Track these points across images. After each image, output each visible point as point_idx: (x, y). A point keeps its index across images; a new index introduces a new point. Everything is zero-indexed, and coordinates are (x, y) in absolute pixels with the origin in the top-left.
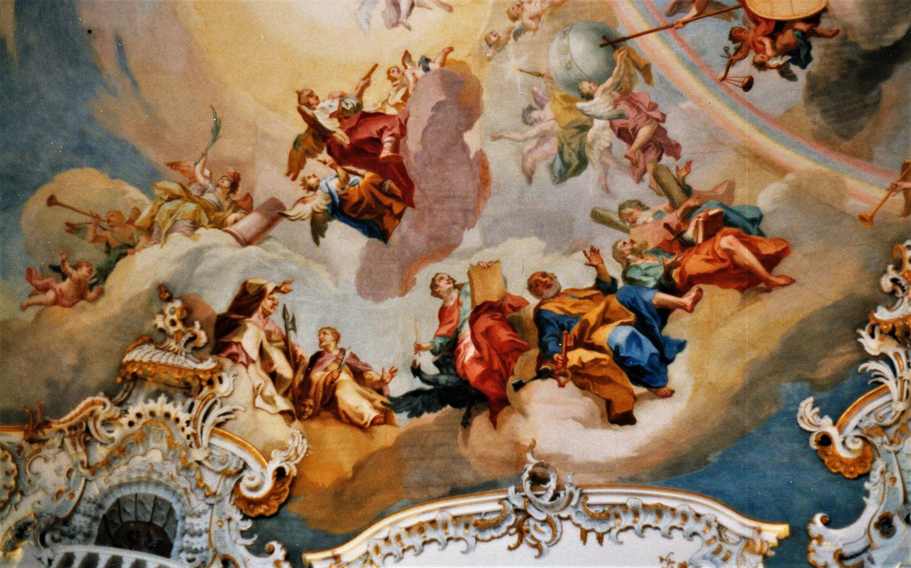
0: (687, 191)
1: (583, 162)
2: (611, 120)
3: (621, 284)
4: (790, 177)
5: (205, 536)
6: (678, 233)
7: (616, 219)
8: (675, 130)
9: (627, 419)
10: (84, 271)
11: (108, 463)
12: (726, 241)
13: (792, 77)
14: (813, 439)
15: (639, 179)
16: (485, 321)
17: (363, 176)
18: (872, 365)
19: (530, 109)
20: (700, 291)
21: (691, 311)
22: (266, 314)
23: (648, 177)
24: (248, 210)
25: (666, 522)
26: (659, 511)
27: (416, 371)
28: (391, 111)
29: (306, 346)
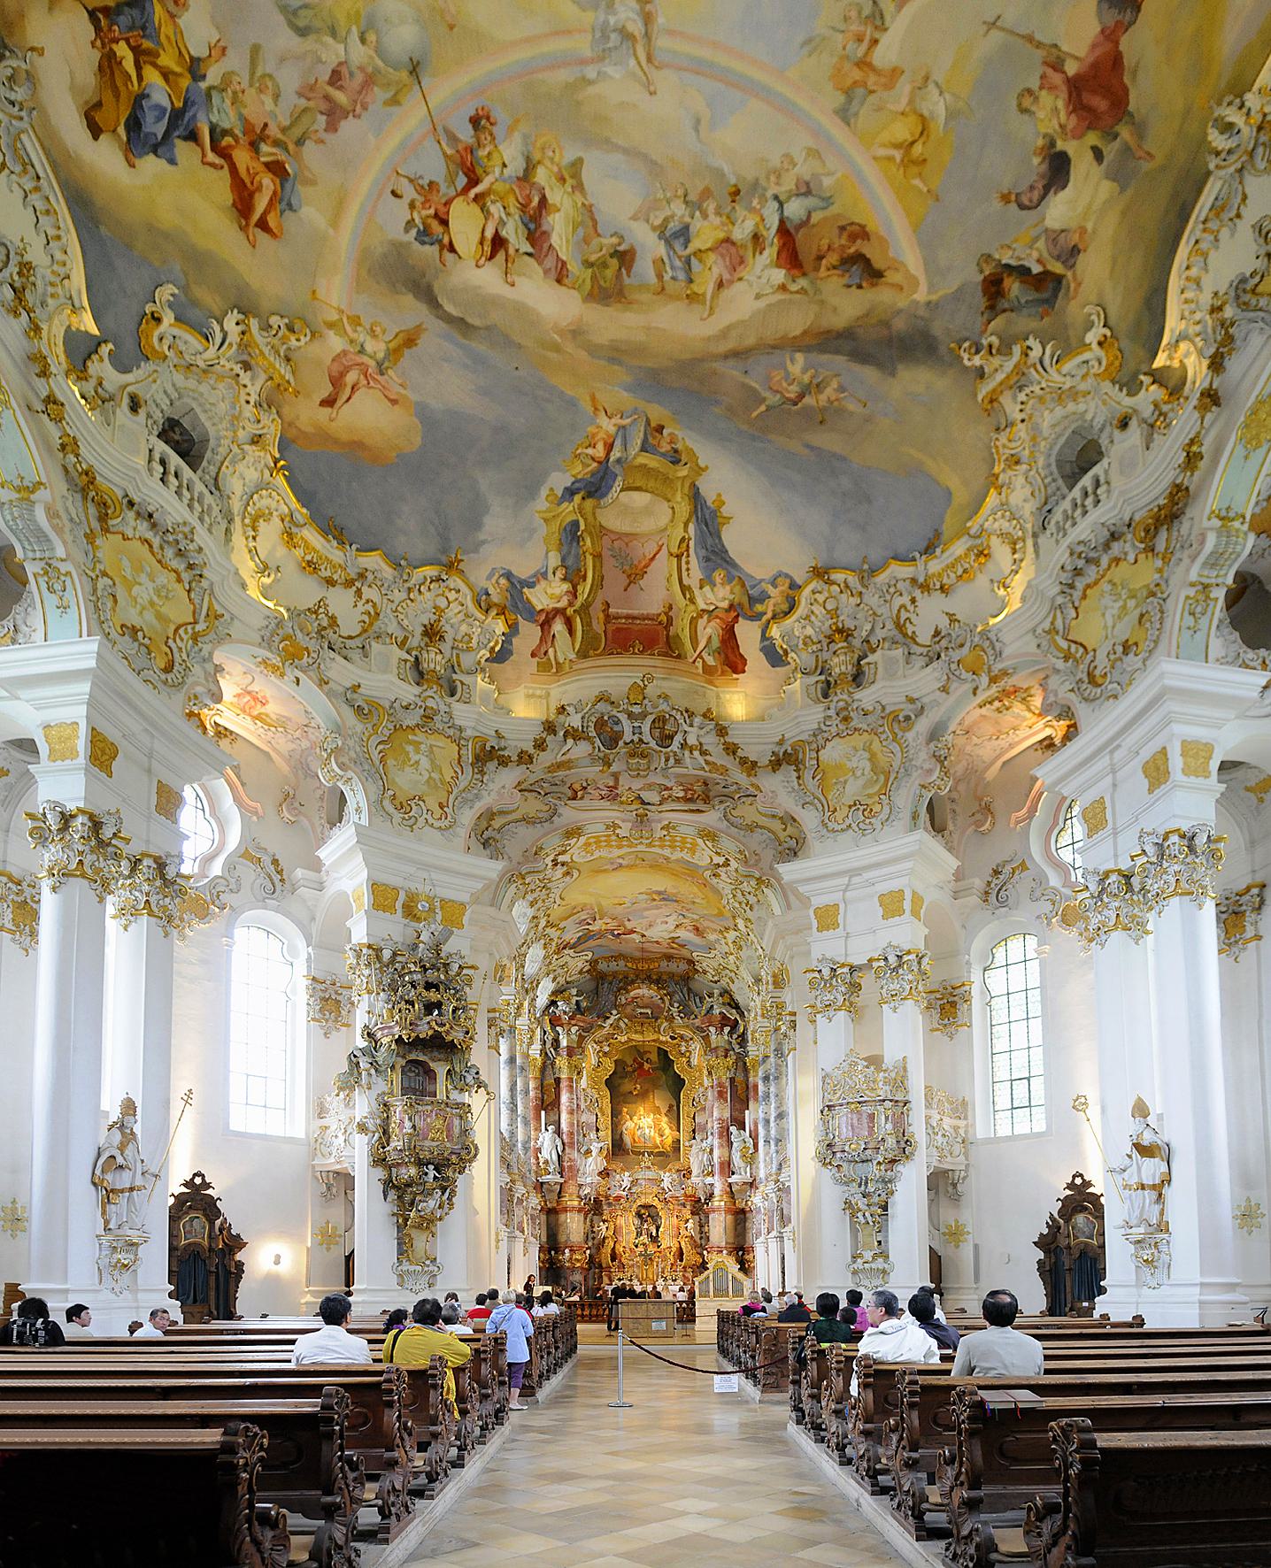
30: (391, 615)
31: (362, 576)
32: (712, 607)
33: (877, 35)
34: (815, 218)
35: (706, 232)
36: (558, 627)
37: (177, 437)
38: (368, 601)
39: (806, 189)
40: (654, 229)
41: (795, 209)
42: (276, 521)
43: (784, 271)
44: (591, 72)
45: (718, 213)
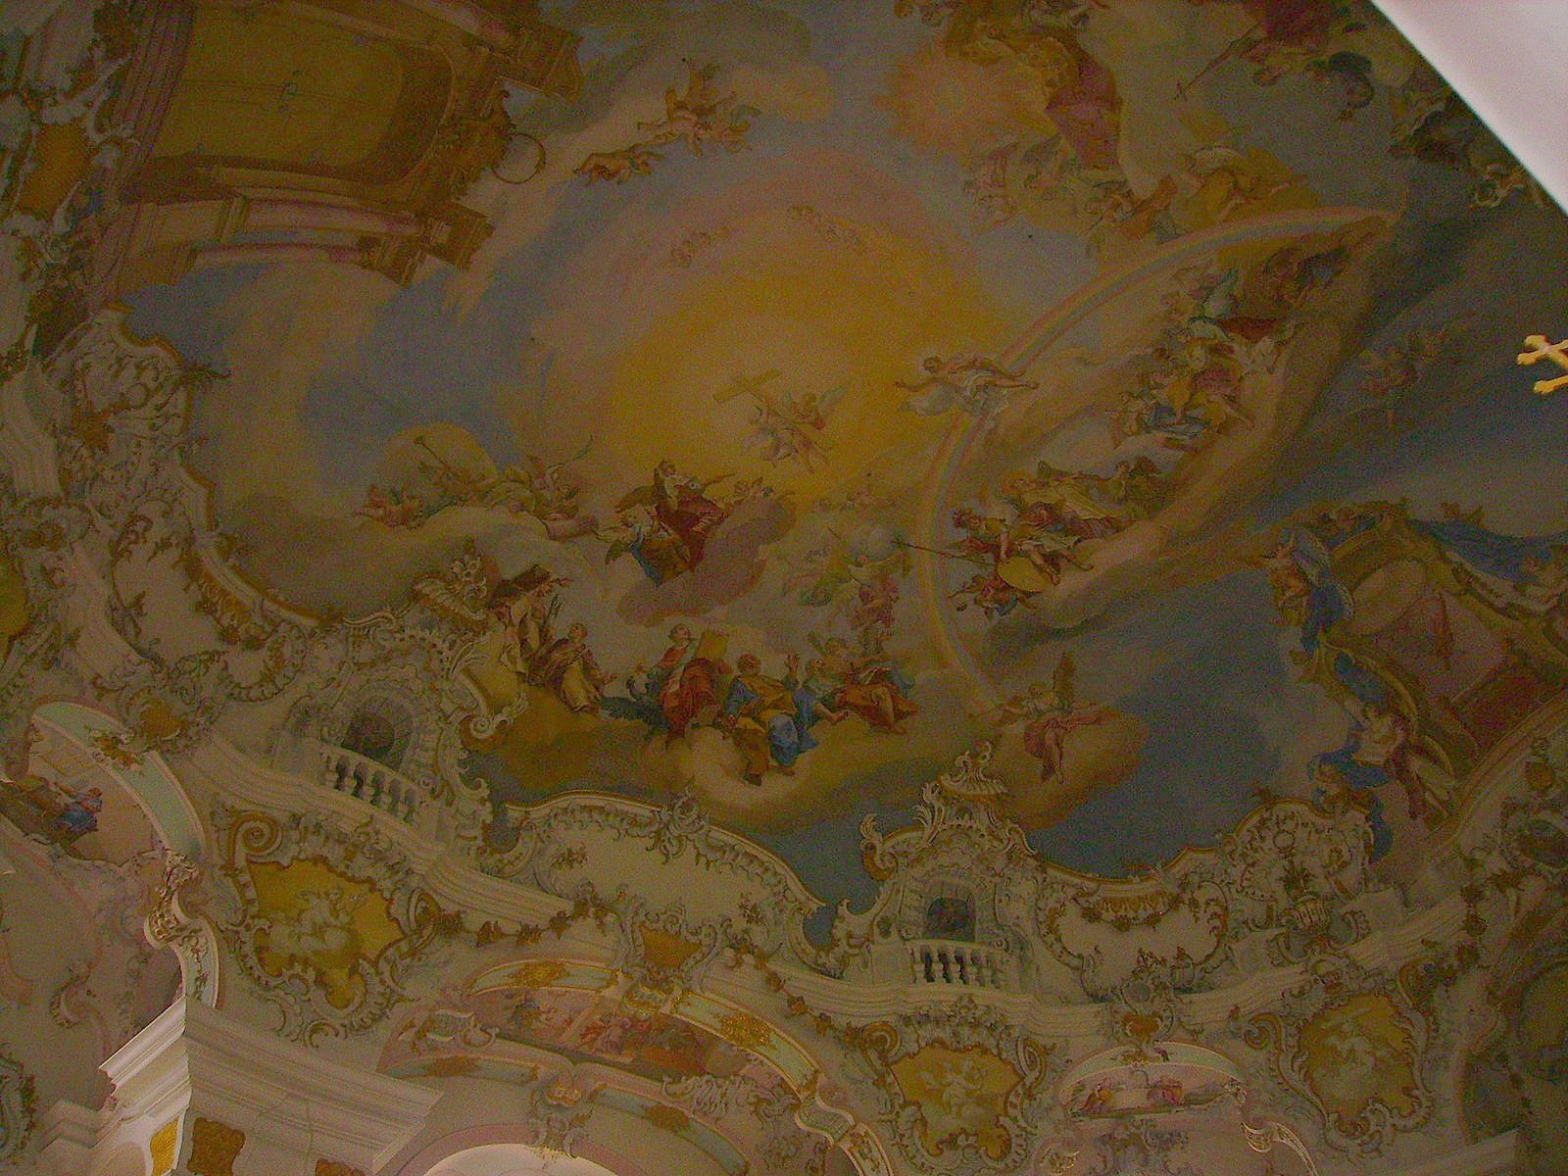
0: (879, 650)
1: (827, 601)
2: (862, 585)
3: (800, 686)
4: (946, 671)
5: (431, 753)
6: (855, 671)
7: (823, 645)
8: (898, 611)
9: (755, 779)
10: (416, 503)
11: (373, 665)
12: (880, 690)
13: (990, 618)
14: (863, 843)
15: (854, 628)
16: (696, 670)
17: (669, 534)
18: (921, 808)
19: (816, 553)
20: (847, 714)
21: (835, 724)
22: (540, 595)
23: (860, 629)
24: (570, 517)
25: (755, 868)
26: (752, 858)
27: (630, 684)
28: (721, 505)
29: (559, 629)
30: (1241, 897)
31: (1183, 885)
32: (1555, 600)
33: (1125, 190)
34: (1237, 291)
35: (1173, 391)
36: (1416, 764)
37: (952, 909)
38: (1208, 904)
39: (1204, 292)
40: (1137, 433)
41: (1215, 307)
42: (1072, 910)
43: (1265, 338)
44: (989, 424)
45: (1167, 376)
